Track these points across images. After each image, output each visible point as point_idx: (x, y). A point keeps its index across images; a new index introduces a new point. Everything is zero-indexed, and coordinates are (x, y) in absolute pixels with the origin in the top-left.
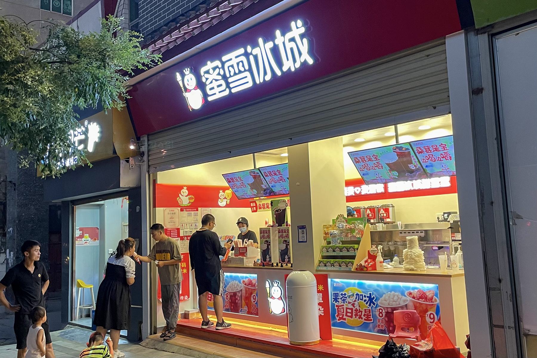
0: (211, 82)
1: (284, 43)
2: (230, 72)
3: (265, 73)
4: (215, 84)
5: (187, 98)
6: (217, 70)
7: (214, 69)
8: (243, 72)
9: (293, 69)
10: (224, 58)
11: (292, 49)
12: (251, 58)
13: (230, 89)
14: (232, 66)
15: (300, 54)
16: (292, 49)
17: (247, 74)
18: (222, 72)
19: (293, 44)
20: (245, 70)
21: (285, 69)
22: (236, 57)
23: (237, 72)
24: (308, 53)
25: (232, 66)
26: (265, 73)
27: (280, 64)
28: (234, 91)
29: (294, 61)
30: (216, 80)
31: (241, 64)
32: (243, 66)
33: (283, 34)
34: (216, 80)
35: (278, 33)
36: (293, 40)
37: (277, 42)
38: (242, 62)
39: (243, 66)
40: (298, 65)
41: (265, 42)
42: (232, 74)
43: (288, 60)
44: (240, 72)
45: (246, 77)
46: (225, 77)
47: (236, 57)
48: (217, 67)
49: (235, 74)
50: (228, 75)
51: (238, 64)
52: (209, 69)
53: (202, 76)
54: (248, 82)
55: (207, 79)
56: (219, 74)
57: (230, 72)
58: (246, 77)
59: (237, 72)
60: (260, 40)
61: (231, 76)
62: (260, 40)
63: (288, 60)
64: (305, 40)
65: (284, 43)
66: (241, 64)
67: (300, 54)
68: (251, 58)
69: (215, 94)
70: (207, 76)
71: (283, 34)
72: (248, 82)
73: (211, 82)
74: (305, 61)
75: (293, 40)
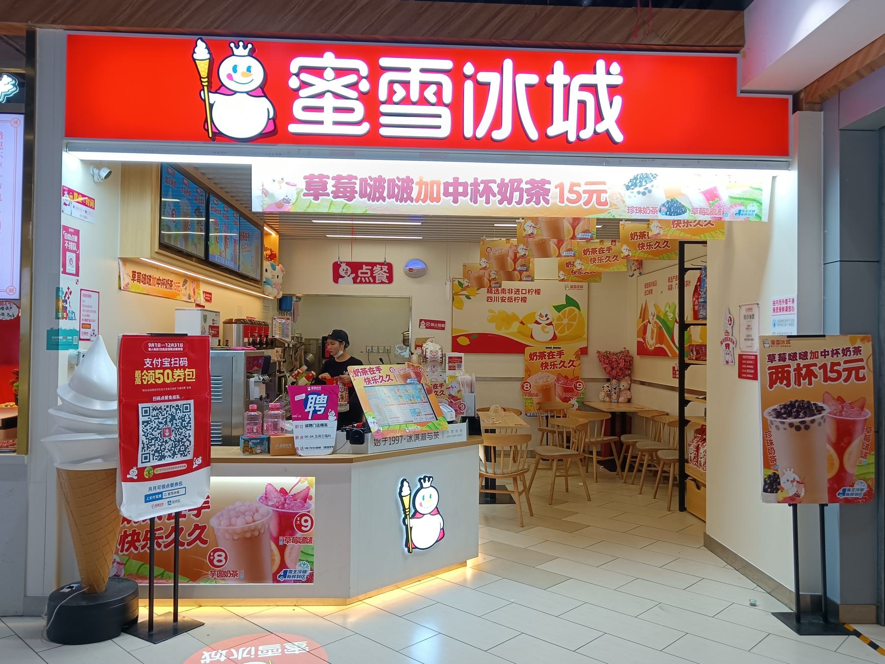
0: (320, 95)
1: (567, 88)
2: (391, 92)
3: (497, 123)
4: (328, 102)
5: (211, 106)
6: (352, 78)
7: (340, 73)
8: (428, 103)
9: (572, 138)
10: (384, 62)
11: (582, 104)
12: (469, 86)
13: (376, 126)
14: (406, 85)
15: (599, 117)
16: (582, 104)
17: (446, 113)
18: (365, 86)
19: (588, 97)
20: (440, 103)
21: (552, 131)
22: (423, 71)
23: (415, 96)
24: (552, 124)
25: (406, 85)
26: (497, 123)
27: (543, 117)
28: (383, 132)
29: (582, 124)
30: (337, 96)
31: (433, 88)
32: (439, 94)
33: (571, 71)
34: (337, 96)
35: (559, 66)
36: (592, 89)
37: (550, 79)
38: (439, 85)
39: (439, 94)
40: (586, 134)
41: (516, 72)
42: (396, 98)
43: (566, 117)
44: (423, 101)
45: (439, 116)
46: (370, 100)
47: (423, 71)
48: (356, 71)
49: (406, 101)
50: (383, 95)
51: (424, 85)
52: (327, 68)
53: (291, 75)
54: (439, 127)
55: (304, 85)
56: (354, 86)
57: (391, 92)
58: (439, 116)
59: (415, 96)
60: (508, 64)
61: (389, 101)
62: (508, 64)
63: (566, 117)
64: (618, 100)
65: (567, 88)
66: (433, 88)
67: (599, 117)
68: (469, 86)
69: (321, 123)
70: (305, 77)
71: (571, 71)
72: (439, 127)
73: (320, 95)
74: (607, 132)
75: (592, 89)
